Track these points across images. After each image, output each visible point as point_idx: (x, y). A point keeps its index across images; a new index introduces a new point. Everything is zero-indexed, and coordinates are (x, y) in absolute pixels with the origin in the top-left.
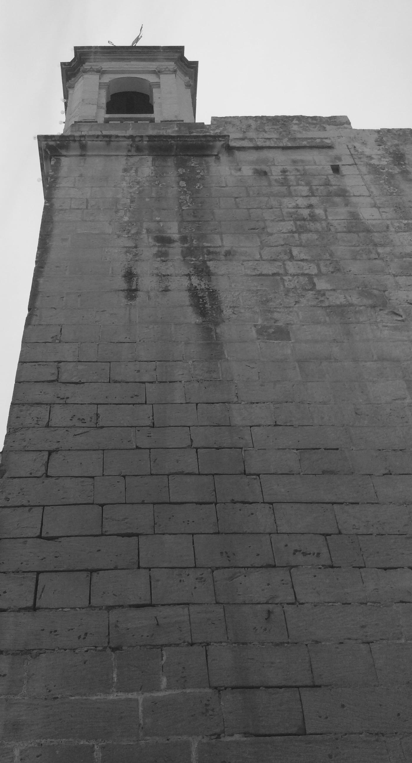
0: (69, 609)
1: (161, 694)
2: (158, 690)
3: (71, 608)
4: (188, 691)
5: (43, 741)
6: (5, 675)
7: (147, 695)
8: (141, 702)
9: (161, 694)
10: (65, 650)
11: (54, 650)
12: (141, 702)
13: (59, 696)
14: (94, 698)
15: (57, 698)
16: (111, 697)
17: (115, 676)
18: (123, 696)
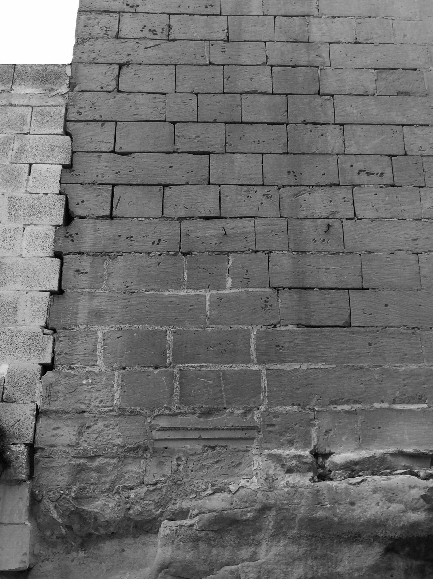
0: (144, 219)
1: (226, 292)
2: (225, 288)
3: (145, 218)
4: (250, 290)
5: (123, 326)
6: (86, 273)
7: (214, 292)
8: (208, 297)
9: (226, 292)
10: (141, 253)
11: (130, 253)
12: (208, 297)
13: (136, 291)
14: (167, 293)
15: (134, 292)
16: (182, 293)
17: (185, 276)
18: (192, 292)
